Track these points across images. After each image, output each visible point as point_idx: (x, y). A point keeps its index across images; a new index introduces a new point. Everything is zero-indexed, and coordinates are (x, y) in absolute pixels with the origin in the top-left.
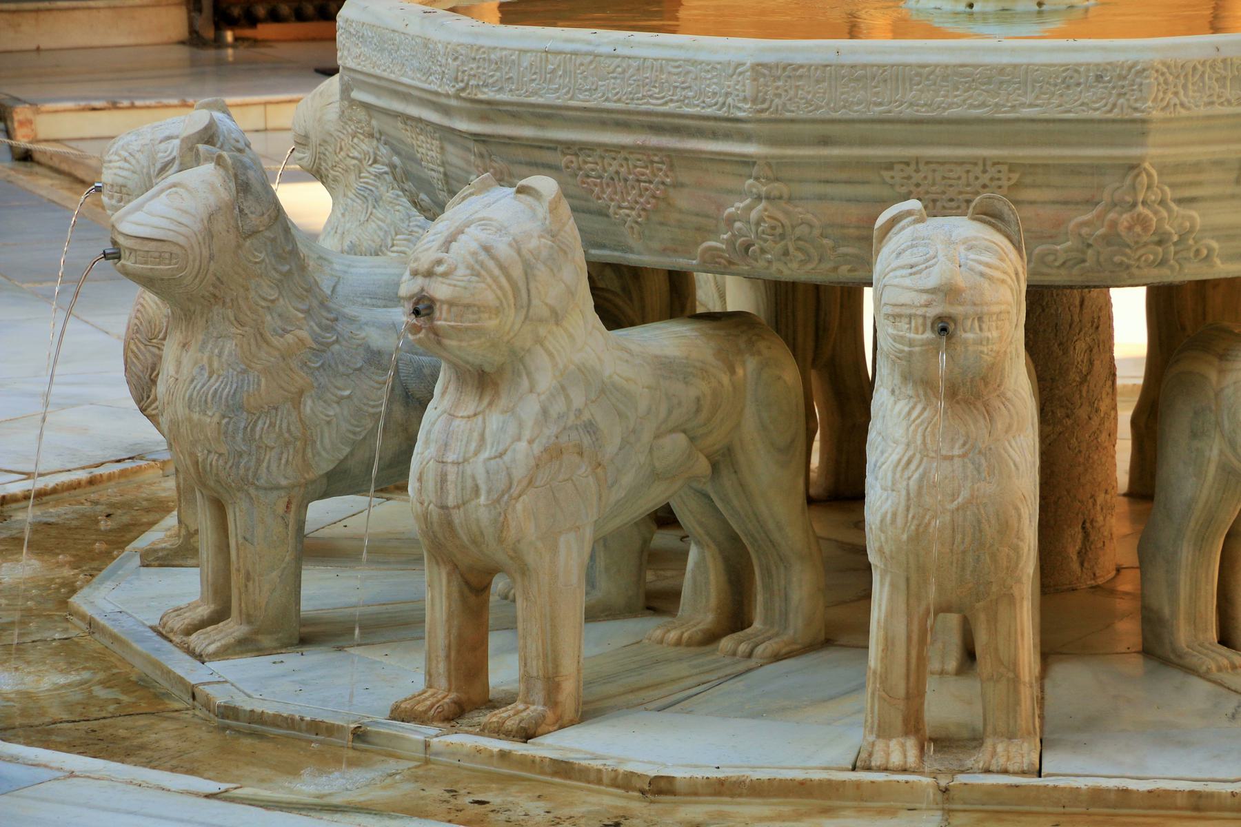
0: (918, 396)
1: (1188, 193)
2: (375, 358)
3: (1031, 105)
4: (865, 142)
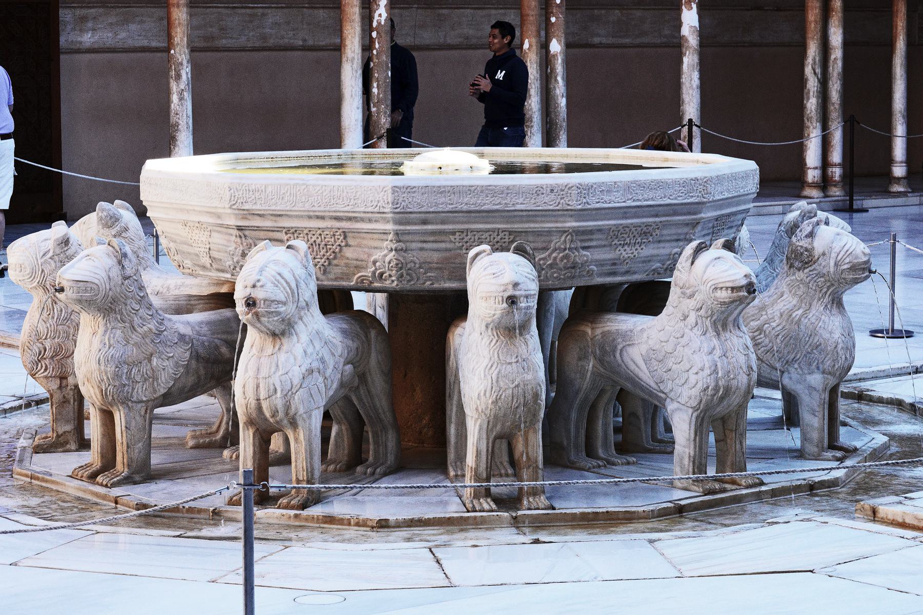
1: (586, 244)
2: (182, 337)
4: (443, 222)
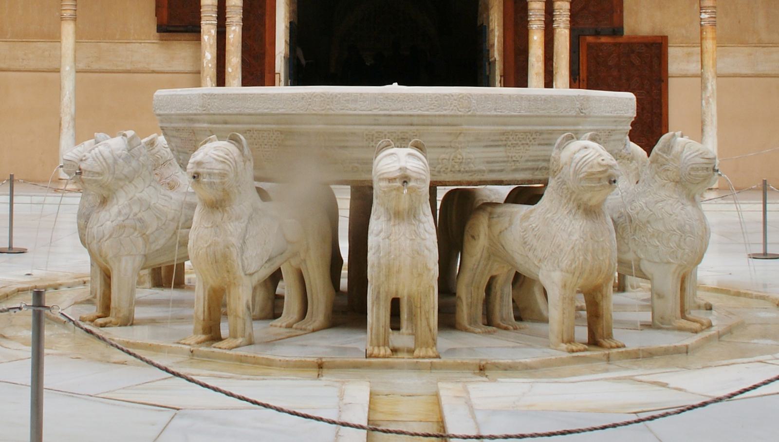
3: (283, 108)
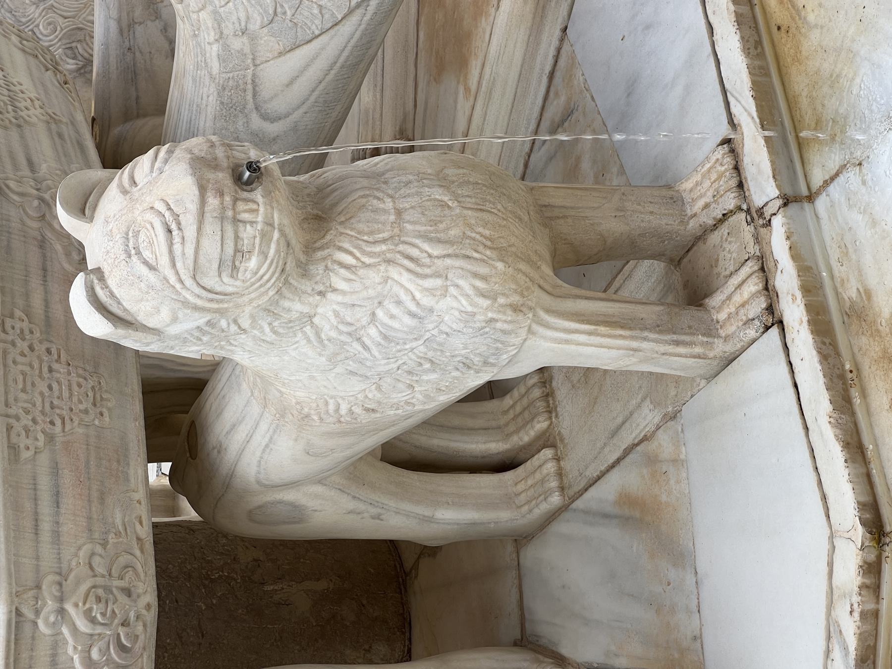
0: (324, 259)
